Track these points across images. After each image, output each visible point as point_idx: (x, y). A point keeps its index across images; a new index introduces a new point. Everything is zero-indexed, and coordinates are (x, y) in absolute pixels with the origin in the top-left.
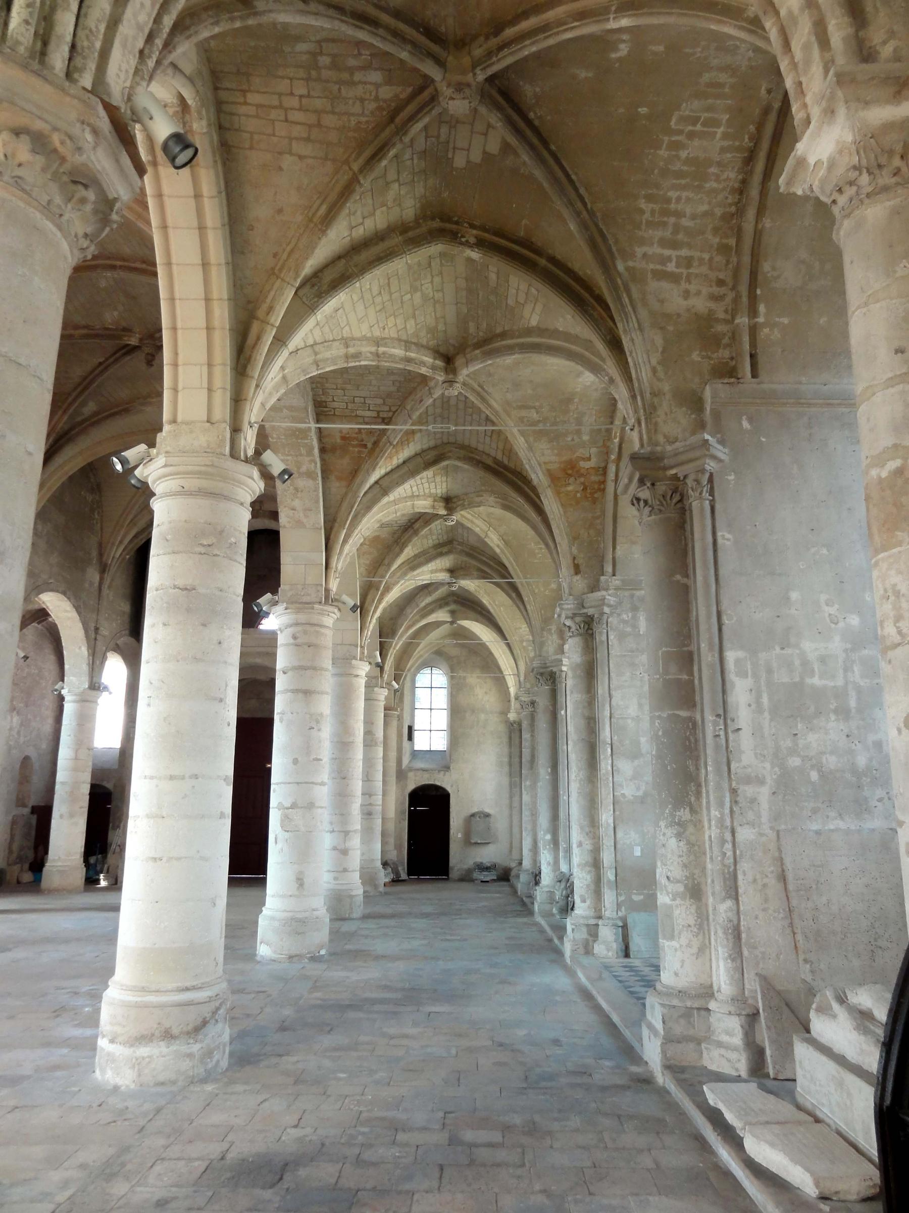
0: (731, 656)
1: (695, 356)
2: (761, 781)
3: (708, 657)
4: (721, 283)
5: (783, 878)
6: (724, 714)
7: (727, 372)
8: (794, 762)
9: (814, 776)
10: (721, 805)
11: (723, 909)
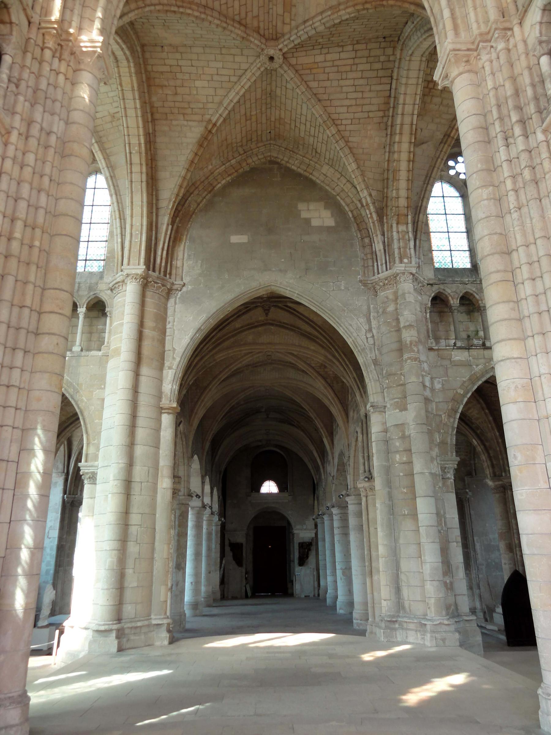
0: (475, 538)
1: (463, 469)
2: (483, 565)
3: (470, 538)
4: (467, 452)
5: (489, 585)
6: (475, 551)
7: (469, 474)
8: (489, 561)
9: (493, 563)
10: (475, 569)
11: (478, 591)
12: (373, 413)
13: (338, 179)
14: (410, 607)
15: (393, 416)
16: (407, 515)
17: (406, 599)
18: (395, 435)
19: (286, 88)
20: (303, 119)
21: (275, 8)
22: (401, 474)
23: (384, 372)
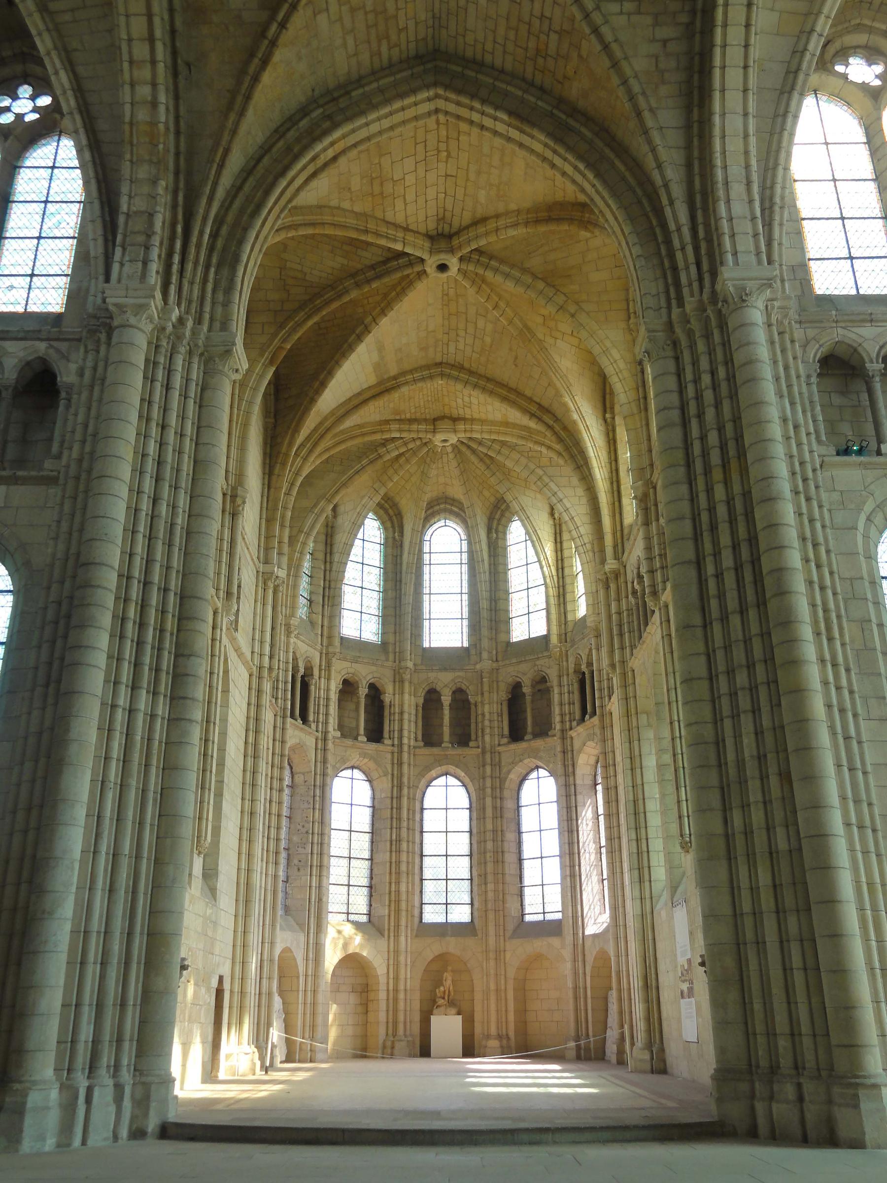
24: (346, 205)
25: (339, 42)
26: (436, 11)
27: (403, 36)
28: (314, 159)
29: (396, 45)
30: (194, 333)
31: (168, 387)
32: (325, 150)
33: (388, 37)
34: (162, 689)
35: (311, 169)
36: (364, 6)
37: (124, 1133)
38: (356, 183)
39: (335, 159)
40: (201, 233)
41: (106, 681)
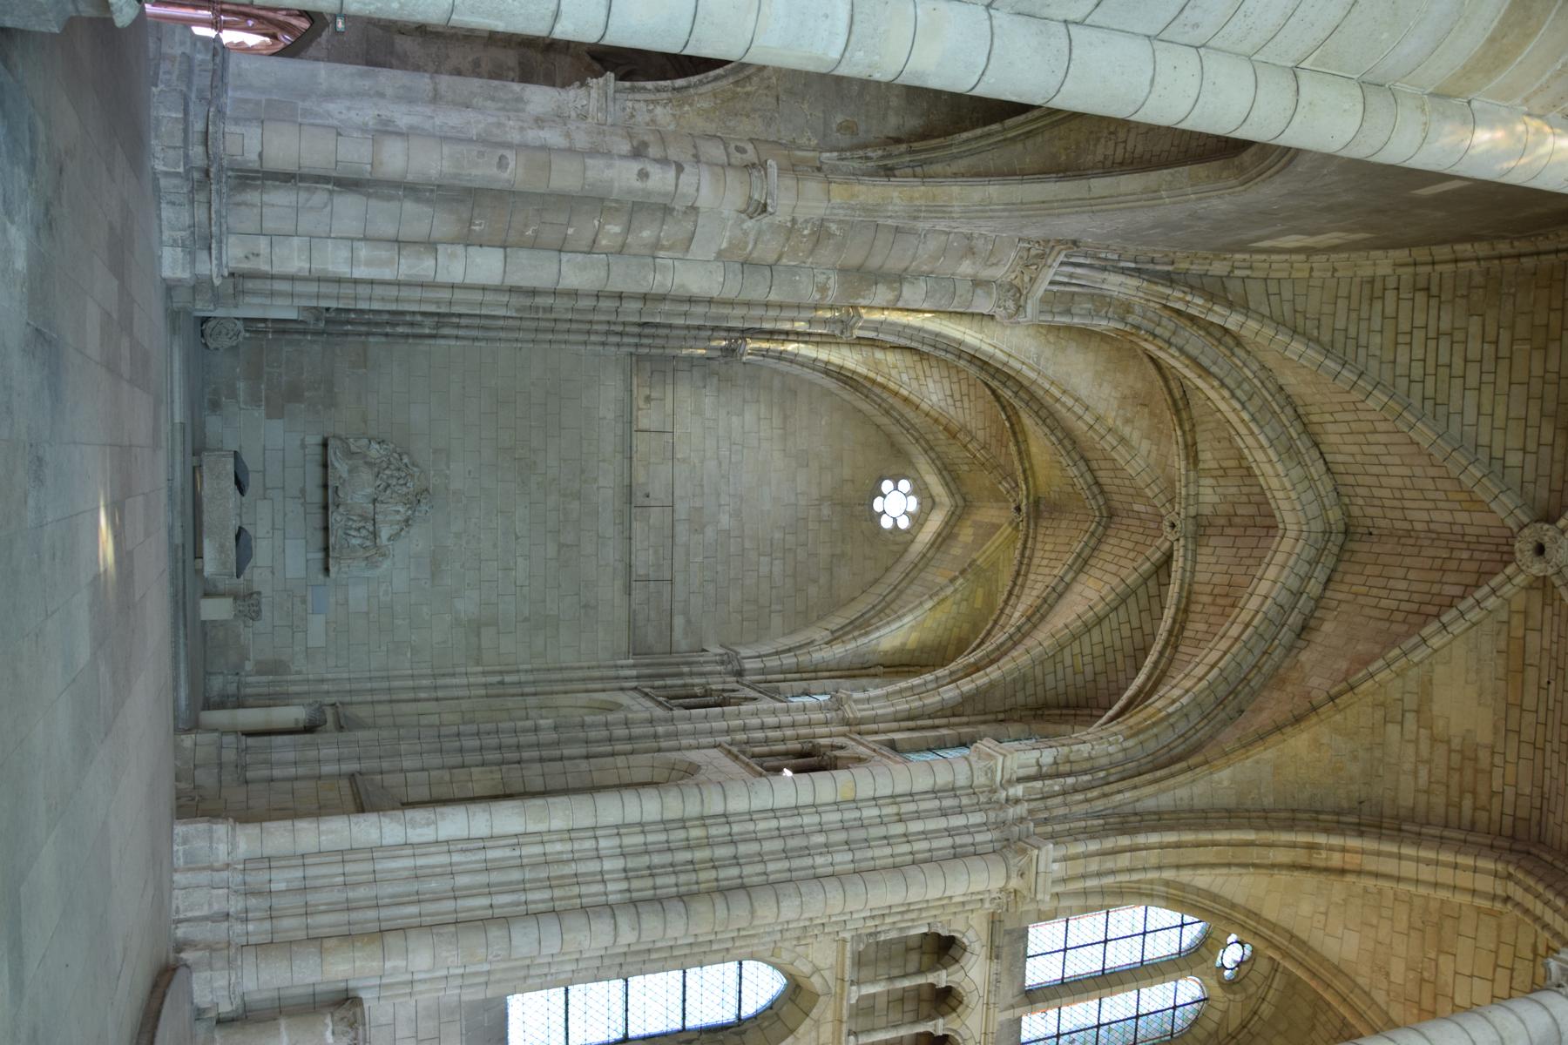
12: (750, 198)
13: (1335, 270)
14: (245, 204)
15: (715, 236)
16: (470, 230)
17: (266, 198)
18: (671, 231)
19: (1524, 450)
20: (1472, 380)
21: (1546, 644)
22: (570, 231)
23: (833, 227)
24: (1380, 997)
25: (1408, 766)
26: (1546, 789)
27: (1496, 801)
28: (1311, 847)
29: (1483, 808)
30: (1022, 820)
31: (944, 813)
32: (1331, 849)
33: (1474, 793)
34: (636, 884)
35: (1301, 856)
36: (1449, 742)
37: (181, 932)
38: (1398, 971)
39: (1343, 872)
40: (1119, 792)
41: (617, 826)
